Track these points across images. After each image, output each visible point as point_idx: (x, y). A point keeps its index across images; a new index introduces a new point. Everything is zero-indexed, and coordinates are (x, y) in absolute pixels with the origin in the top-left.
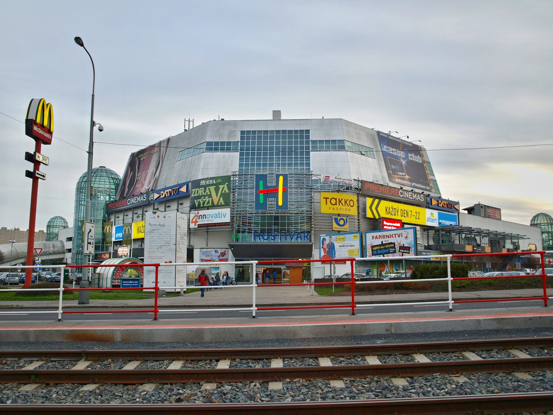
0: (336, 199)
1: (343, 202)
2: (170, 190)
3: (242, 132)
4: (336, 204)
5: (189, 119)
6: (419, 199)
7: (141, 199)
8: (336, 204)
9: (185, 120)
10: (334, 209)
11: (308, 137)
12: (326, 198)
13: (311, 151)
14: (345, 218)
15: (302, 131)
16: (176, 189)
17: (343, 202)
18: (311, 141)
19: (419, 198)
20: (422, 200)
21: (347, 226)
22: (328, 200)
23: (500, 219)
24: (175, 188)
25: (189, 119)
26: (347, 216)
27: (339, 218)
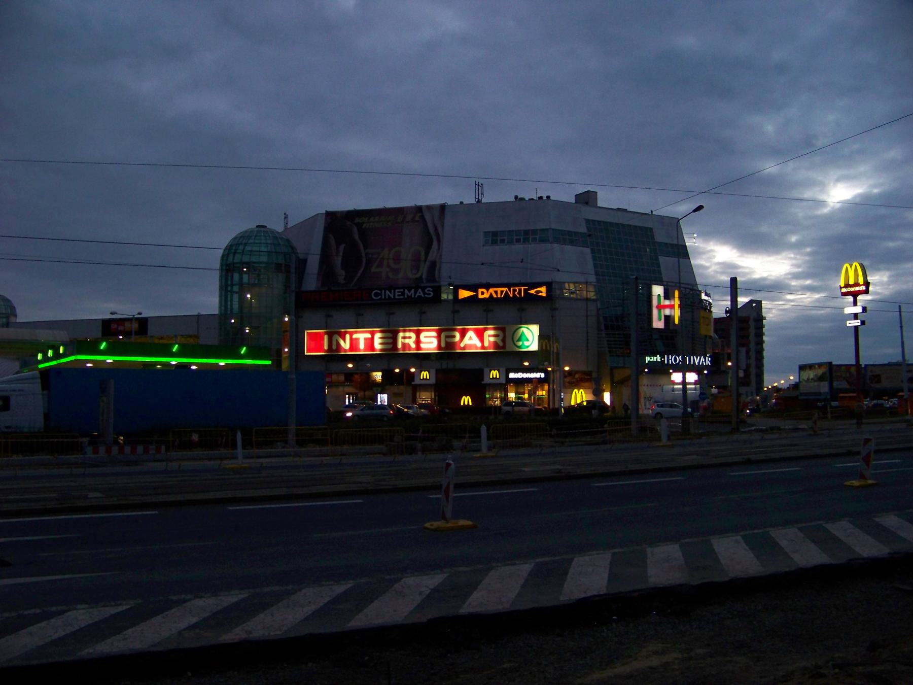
2: (505, 289)
3: (588, 221)
7: (418, 294)
16: (520, 290)
24: (517, 288)
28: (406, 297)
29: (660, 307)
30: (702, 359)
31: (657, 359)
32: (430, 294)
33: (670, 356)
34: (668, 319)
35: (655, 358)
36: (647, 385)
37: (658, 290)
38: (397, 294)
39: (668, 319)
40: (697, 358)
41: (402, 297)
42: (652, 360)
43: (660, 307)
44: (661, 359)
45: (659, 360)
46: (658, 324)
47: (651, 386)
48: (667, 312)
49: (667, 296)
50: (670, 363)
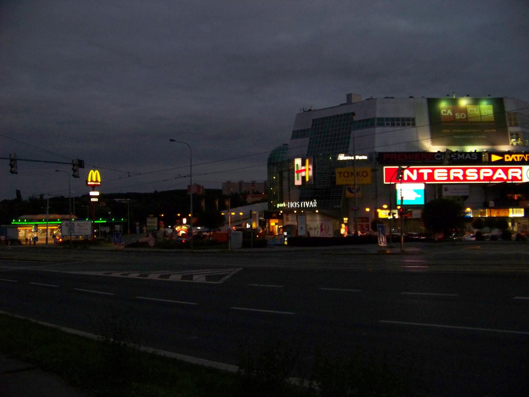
0: (348, 173)
4: (348, 176)
6: (468, 159)
8: (348, 176)
12: (340, 173)
19: (469, 157)
29: (299, 172)
30: (308, 205)
31: (283, 205)
32: (474, 157)
34: (304, 178)
35: (283, 204)
36: (291, 221)
37: (298, 162)
39: (304, 178)
40: (307, 203)
42: (281, 206)
43: (299, 172)
44: (286, 205)
45: (285, 206)
46: (298, 182)
47: (293, 221)
48: (303, 174)
49: (303, 164)
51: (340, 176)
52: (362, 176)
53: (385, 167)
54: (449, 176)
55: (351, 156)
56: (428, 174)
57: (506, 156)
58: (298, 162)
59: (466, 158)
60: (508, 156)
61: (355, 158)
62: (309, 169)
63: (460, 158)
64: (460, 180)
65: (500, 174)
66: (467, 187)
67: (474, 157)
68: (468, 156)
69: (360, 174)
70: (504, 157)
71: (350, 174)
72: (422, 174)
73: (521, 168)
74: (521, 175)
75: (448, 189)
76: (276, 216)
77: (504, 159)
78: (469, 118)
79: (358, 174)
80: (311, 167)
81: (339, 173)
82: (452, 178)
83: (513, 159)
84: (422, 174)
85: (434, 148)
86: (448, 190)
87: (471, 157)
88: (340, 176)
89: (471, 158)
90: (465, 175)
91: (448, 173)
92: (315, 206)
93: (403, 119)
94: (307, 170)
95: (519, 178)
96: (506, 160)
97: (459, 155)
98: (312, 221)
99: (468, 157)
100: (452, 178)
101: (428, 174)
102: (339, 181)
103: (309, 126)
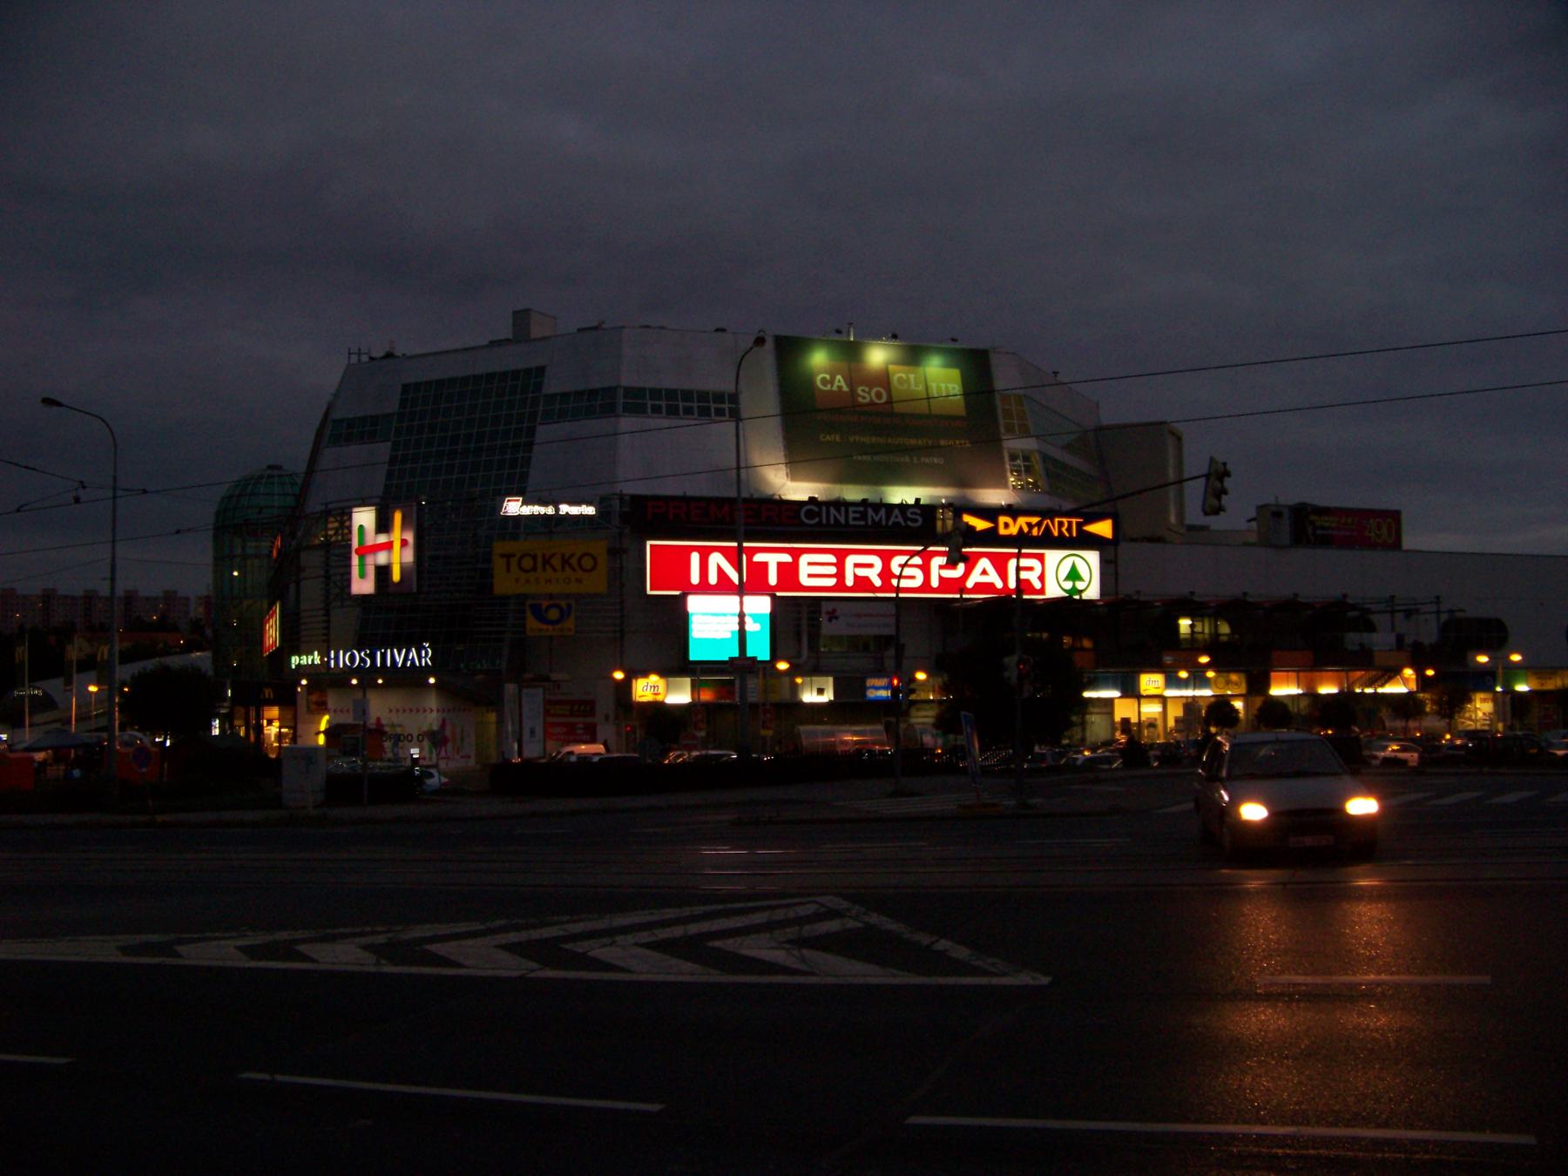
0: (534, 558)
1: (556, 562)
4: (534, 569)
5: (360, 350)
6: (897, 524)
8: (534, 569)
9: (350, 354)
10: (528, 581)
11: (539, 387)
12: (508, 556)
13: (540, 424)
14: (563, 604)
15: (528, 372)
17: (556, 562)
18: (546, 396)
19: (900, 520)
20: (919, 523)
21: (570, 624)
22: (514, 561)
23: (1396, 545)
25: (360, 350)
26: (568, 596)
27: (545, 604)
28: (870, 523)
29: (365, 551)
30: (400, 660)
31: (313, 660)
33: (341, 652)
34: (383, 572)
35: (310, 658)
37: (364, 517)
38: (851, 515)
39: (383, 572)
40: (400, 654)
41: (862, 523)
42: (304, 662)
43: (365, 551)
44: (321, 660)
45: (317, 661)
46: (363, 585)
47: (341, 711)
48: (382, 558)
49: (383, 525)
50: (423, 664)
51: (508, 570)
52: (577, 568)
53: (649, 543)
54: (840, 575)
55: (545, 504)
56: (780, 565)
57: (1002, 519)
58: (364, 517)
59: (890, 523)
60: (1009, 520)
61: (557, 510)
62: (404, 543)
63: (873, 520)
64: (874, 589)
65: (984, 572)
66: (892, 609)
67: (916, 521)
68: (896, 517)
69: (574, 561)
70: (995, 522)
71: (540, 560)
72: (765, 565)
73: (1041, 558)
74: (1042, 578)
75: (837, 614)
76: (272, 696)
77: (995, 529)
78: (896, 402)
79: (565, 562)
80: (410, 537)
81: (503, 556)
82: (849, 582)
83: (1021, 529)
84: (765, 565)
85: (798, 490)
86: (837, 618)
87: (906, 519)
88: (508, 570)
89: (905, 522)
90: (886, 574)
91: (840, 565)
92: (426, 662)
93: (703, 396)
94: (397, 545)
95: (1037, 585)
96: (1002, 531)
97: (870, 511)
98: (404, 711)
99: (896, 520)
100: (849, 582)
101: (780, 565)
102: (505, 583)
103: (393, 406)
